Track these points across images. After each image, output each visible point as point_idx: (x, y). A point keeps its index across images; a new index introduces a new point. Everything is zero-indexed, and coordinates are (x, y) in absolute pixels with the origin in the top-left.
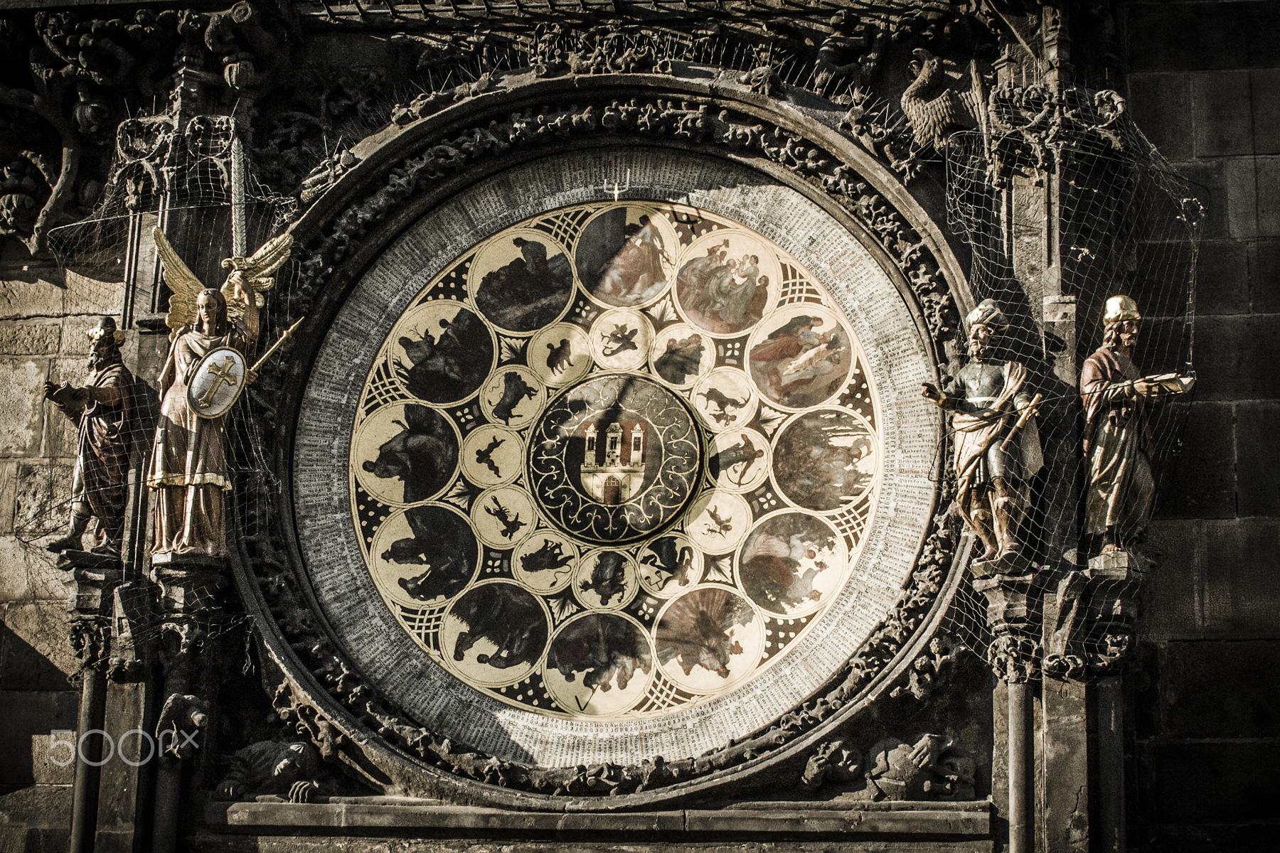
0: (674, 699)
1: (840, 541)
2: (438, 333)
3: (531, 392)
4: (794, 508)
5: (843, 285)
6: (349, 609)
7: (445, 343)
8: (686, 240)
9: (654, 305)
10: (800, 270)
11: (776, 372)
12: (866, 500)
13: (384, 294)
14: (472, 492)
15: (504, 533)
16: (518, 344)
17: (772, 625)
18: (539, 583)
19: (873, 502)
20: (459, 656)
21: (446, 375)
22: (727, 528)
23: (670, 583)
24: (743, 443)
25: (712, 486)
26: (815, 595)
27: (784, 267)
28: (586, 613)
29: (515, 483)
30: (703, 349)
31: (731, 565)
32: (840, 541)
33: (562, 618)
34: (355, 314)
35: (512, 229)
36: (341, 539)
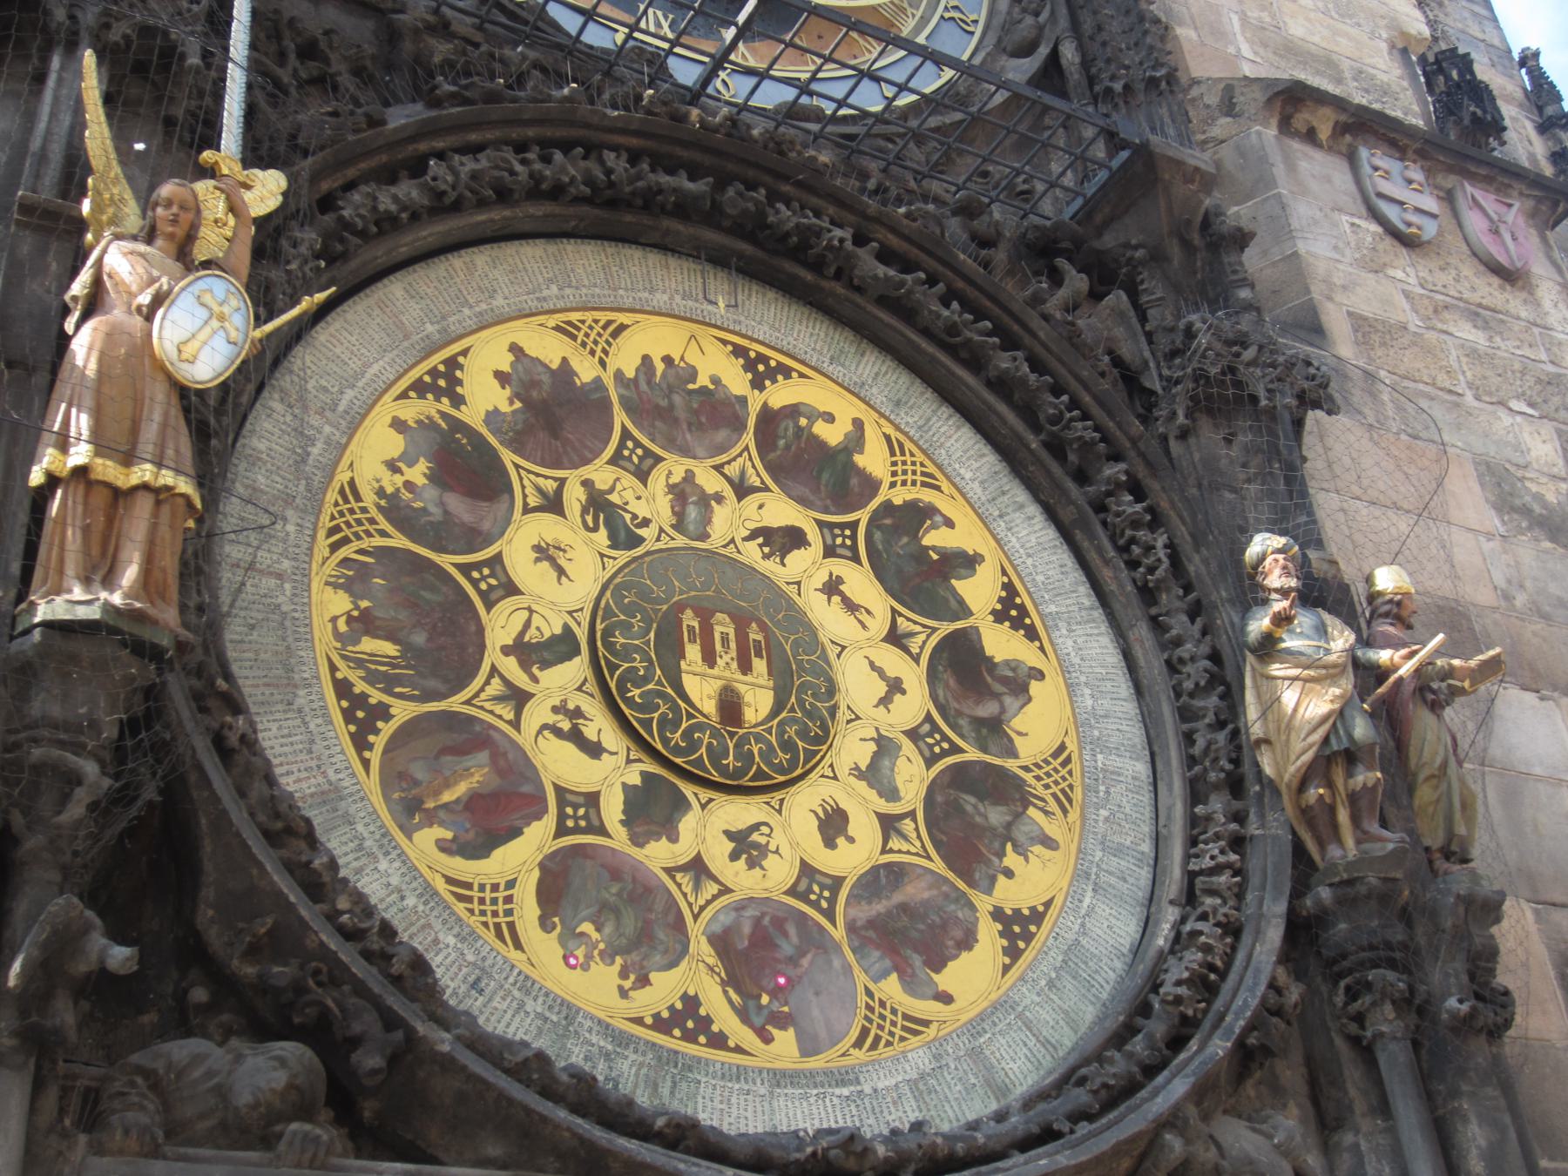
0: (578, 329)
1: (369, 499)
2: (1011, 859)
4: (446, 561)
5: (411, 901)
6: (1004, 493)
7: (997, 845)
8: (691, 1002)
9: (715, 897)
10: (490, 936)
11: (501, 773)
12: (334, 547)
13: (1103, 910)
14: (895, 638)
16: (895, 843)
17: (458, 401)
18: (780, 511)
19: (323, 543)
20: (858, 424)
21: (981, 799)
22: (537, 548)
23: (606, 487)
25: (570, 613)
26: (398, 425)
27: (518, 945)
28: (711, 462)
29: (844, 648)
30: (621, 821)
31: (525, 496)
32: (369, 499)
33: (740, 460)
34: (1131, 880)
35: (964, 1018)
36: (1040, 578)
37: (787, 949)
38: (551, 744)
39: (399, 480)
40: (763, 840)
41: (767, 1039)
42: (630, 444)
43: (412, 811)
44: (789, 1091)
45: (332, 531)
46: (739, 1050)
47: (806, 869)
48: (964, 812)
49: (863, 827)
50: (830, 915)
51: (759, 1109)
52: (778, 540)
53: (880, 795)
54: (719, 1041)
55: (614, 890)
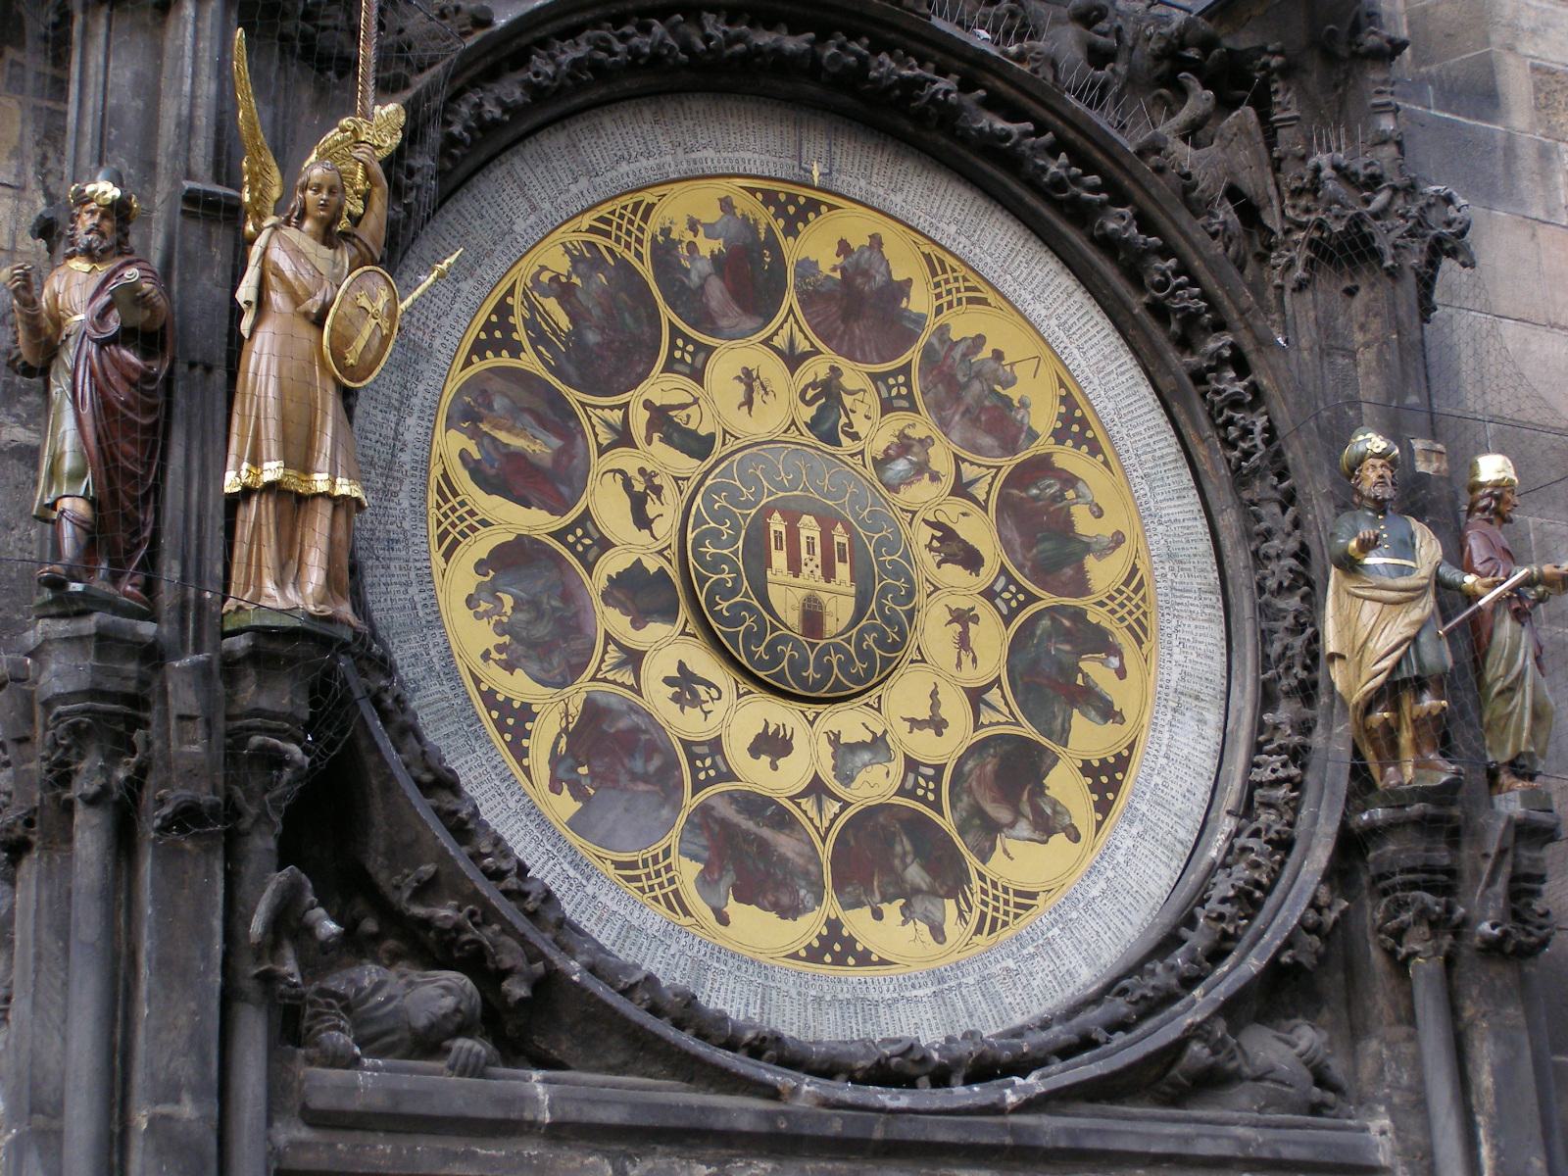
1: (653, 226)
2: (892, 910)
3: (834, 739)
4: (666, 313)
6: (1197, 698)
7: (891, 890)
8: (526, 713)
9: (623, 685)
10: (434, 532)
12: (592, 230)
14: (976, 697)
15: (976, 619)
16: (808, 804)
17: (791, 231)
18: (979, 530)
19: (587, 221)
20: (1118, 539)
22: (747, 372)
24: (656, 436)
25: (725, 432)
26: (726, 205)
27: (447, 556)
29: (923, 661)
30: (610, 578)
31: (776, 333)
32: (653, 226)
33: (984, 471)
35: (720, 942)
37: (638, 765)
40: (704, 696)
41: (555, 787)
42: (901, 379)
43: (467, 416)
44: (532, 827)
45: (601, 219)
46: (527, 771)
47: (716, 745)
48: (891, 847)
50: (698, 786)
51: (497, 810)
52: (954, 547)
53: (834, 768)
54: (520, 753)
55: (554, 603)
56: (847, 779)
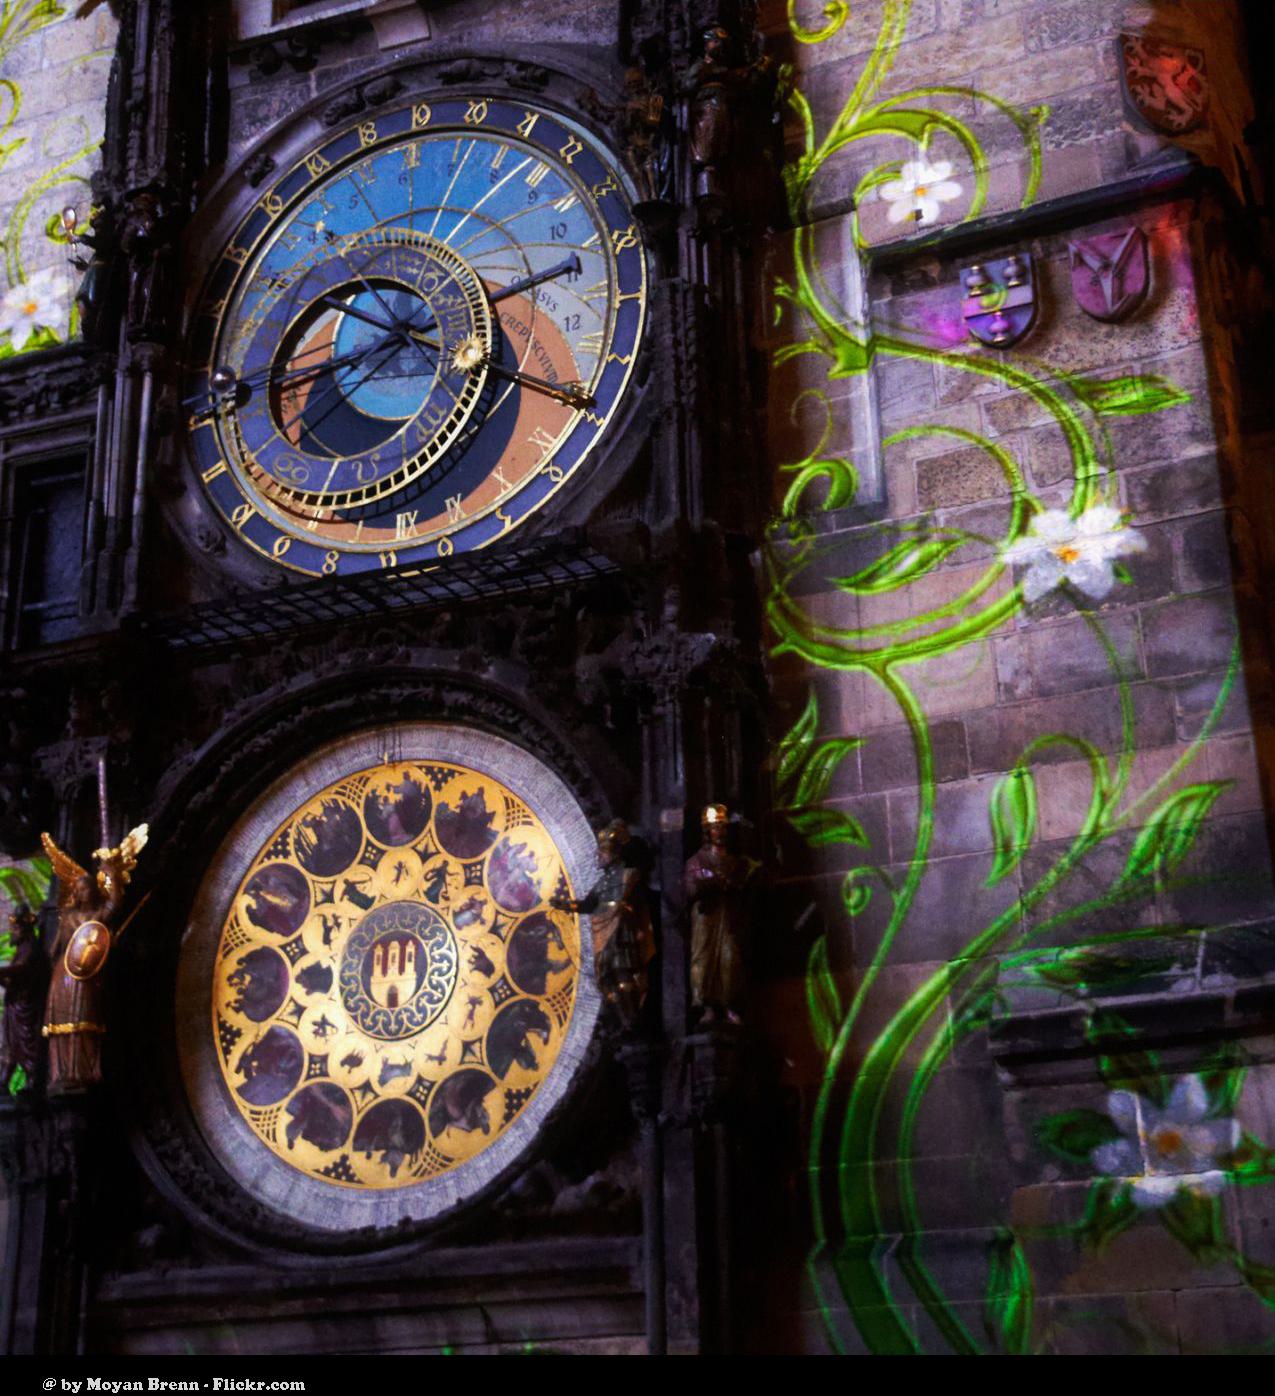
1: (368, 789)
2: (377, 1155)
4: (366, 834)
8: (238, 1033)
12: (337, 793)
14: (467, 1047)
15: (480, 1003)
16: (358, 1094)
17: (438, 788)
26: (406, 776)
32: (368, 789)
38: (319, 922)
39: (385, 793)
41: (238, 1071)
46: (227, 1061)
47: (324, 1059)
49: (358, 1076)
50: (309, 1077)
54: (227, 1051)
56: (383, 1081)
